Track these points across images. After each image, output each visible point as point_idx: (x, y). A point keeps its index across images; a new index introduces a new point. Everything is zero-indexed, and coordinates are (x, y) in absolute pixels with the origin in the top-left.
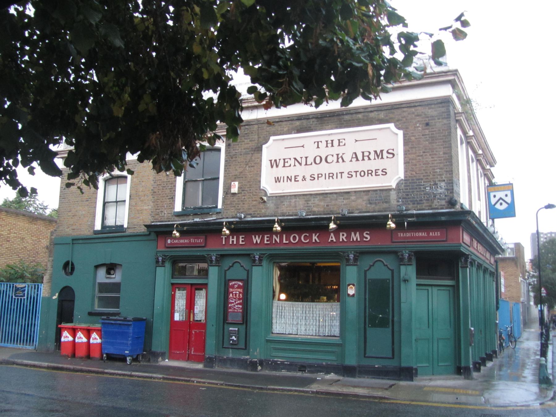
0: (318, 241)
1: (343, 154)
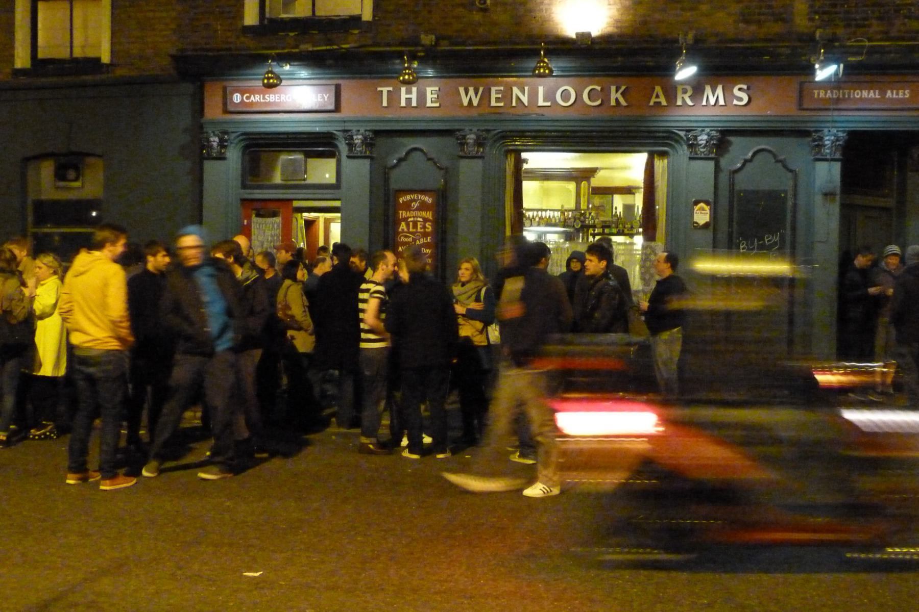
0: (623, 102)
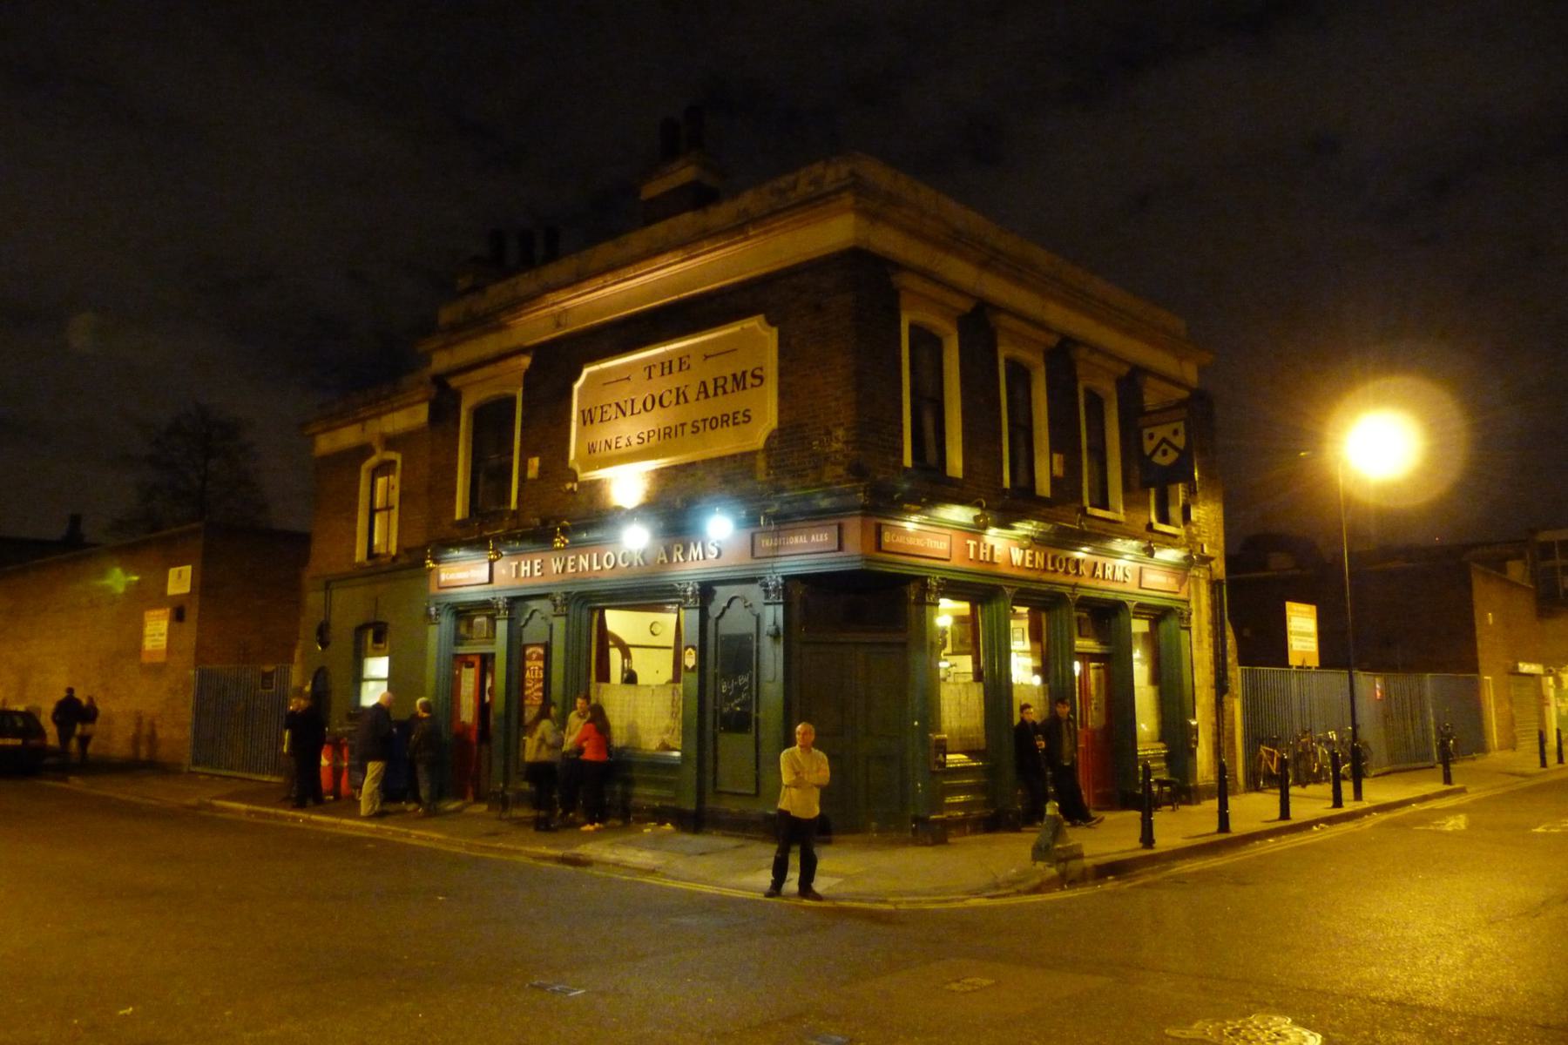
1: (686, 386)
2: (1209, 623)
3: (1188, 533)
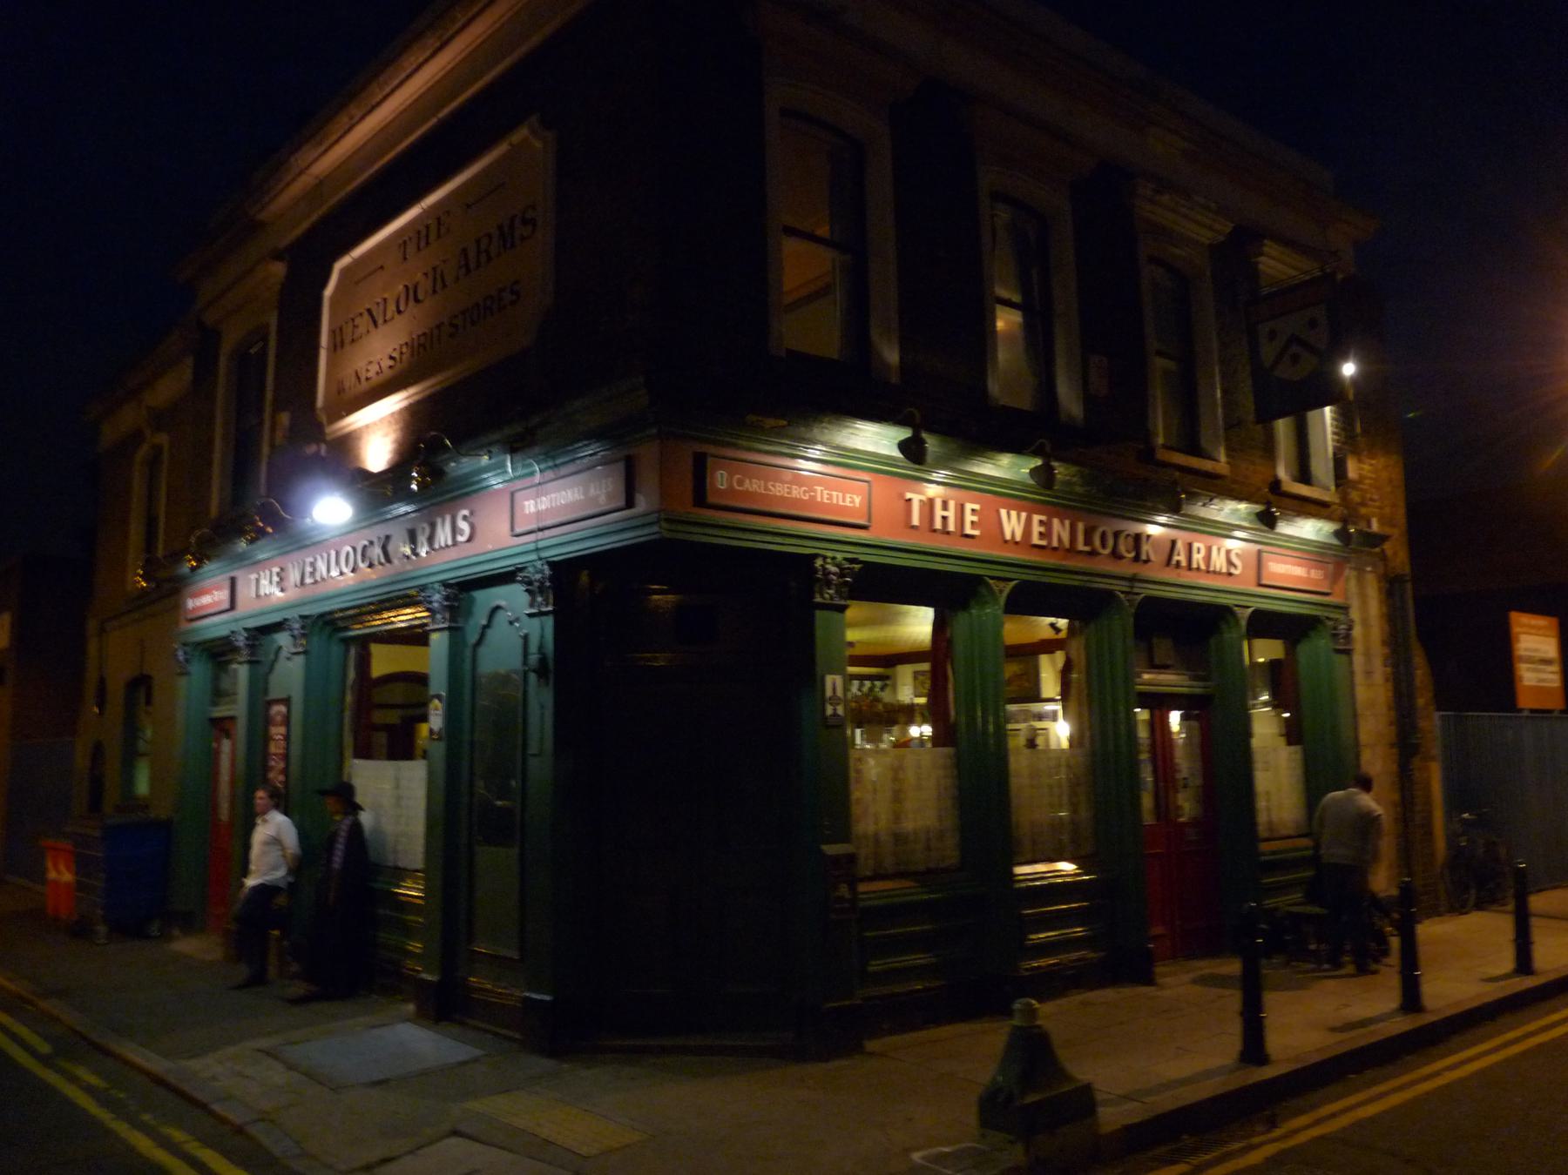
2: (1384, 643)
3: (1344, 499)
